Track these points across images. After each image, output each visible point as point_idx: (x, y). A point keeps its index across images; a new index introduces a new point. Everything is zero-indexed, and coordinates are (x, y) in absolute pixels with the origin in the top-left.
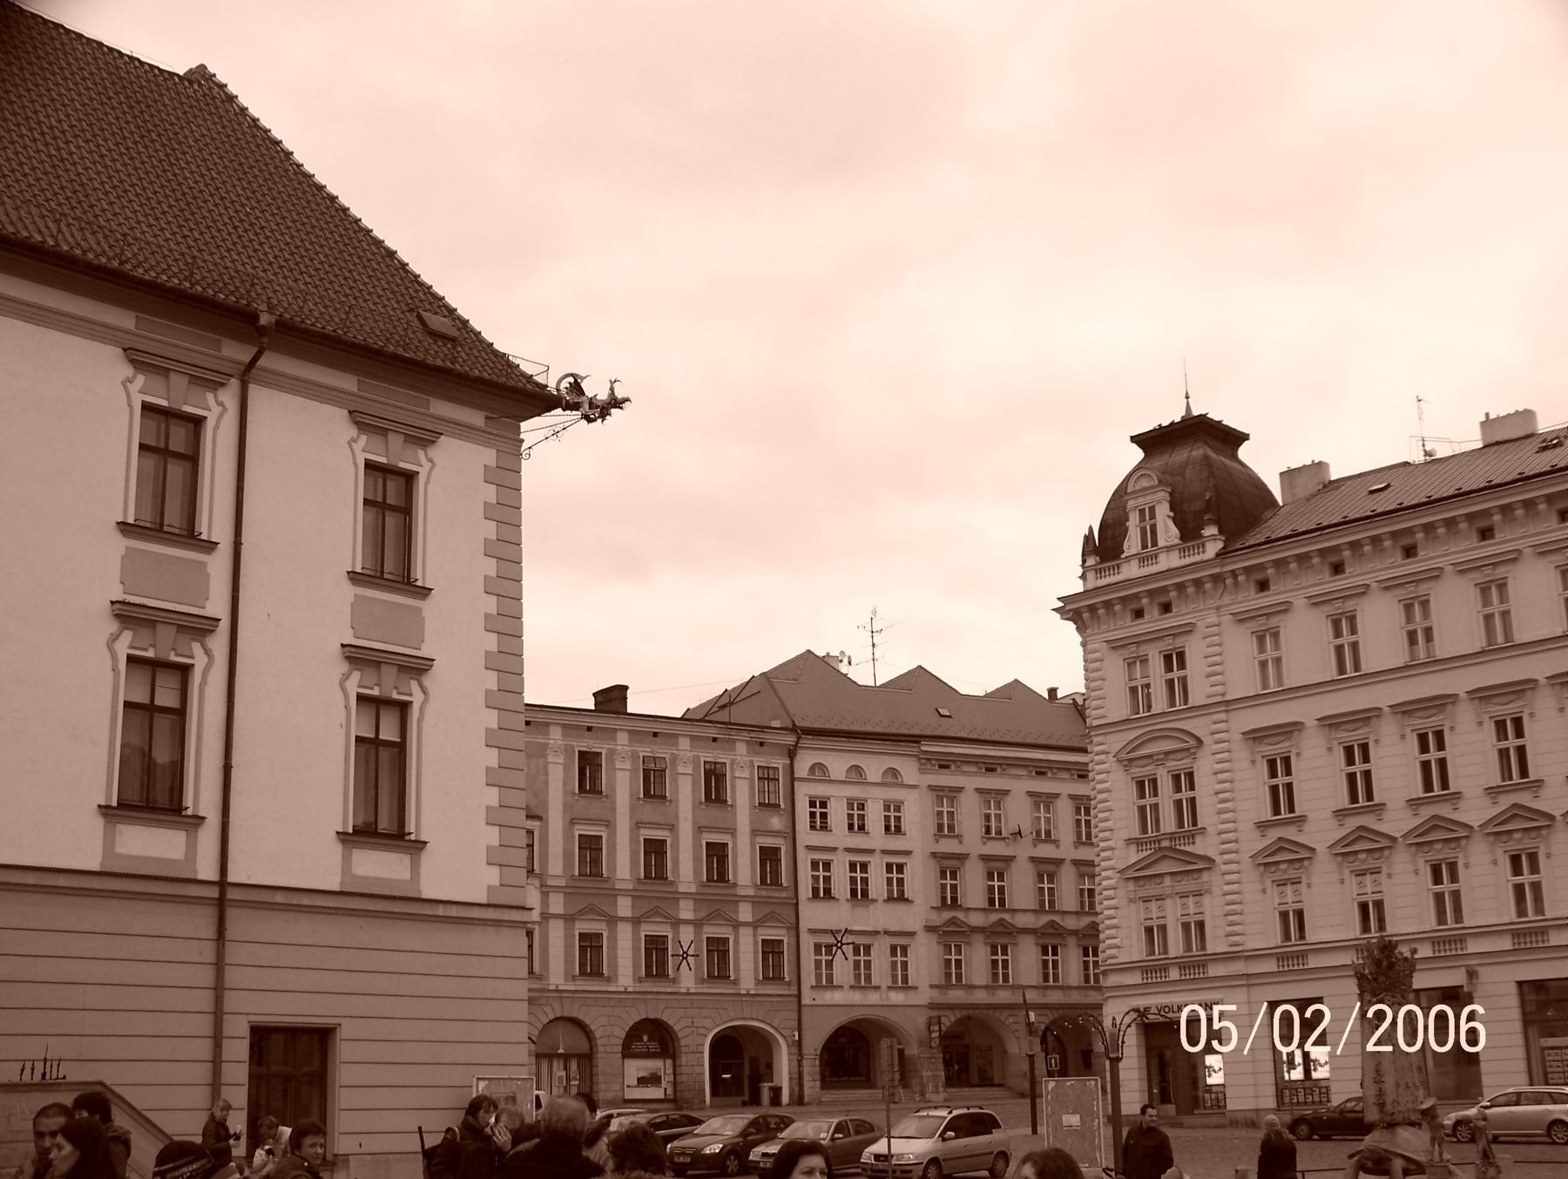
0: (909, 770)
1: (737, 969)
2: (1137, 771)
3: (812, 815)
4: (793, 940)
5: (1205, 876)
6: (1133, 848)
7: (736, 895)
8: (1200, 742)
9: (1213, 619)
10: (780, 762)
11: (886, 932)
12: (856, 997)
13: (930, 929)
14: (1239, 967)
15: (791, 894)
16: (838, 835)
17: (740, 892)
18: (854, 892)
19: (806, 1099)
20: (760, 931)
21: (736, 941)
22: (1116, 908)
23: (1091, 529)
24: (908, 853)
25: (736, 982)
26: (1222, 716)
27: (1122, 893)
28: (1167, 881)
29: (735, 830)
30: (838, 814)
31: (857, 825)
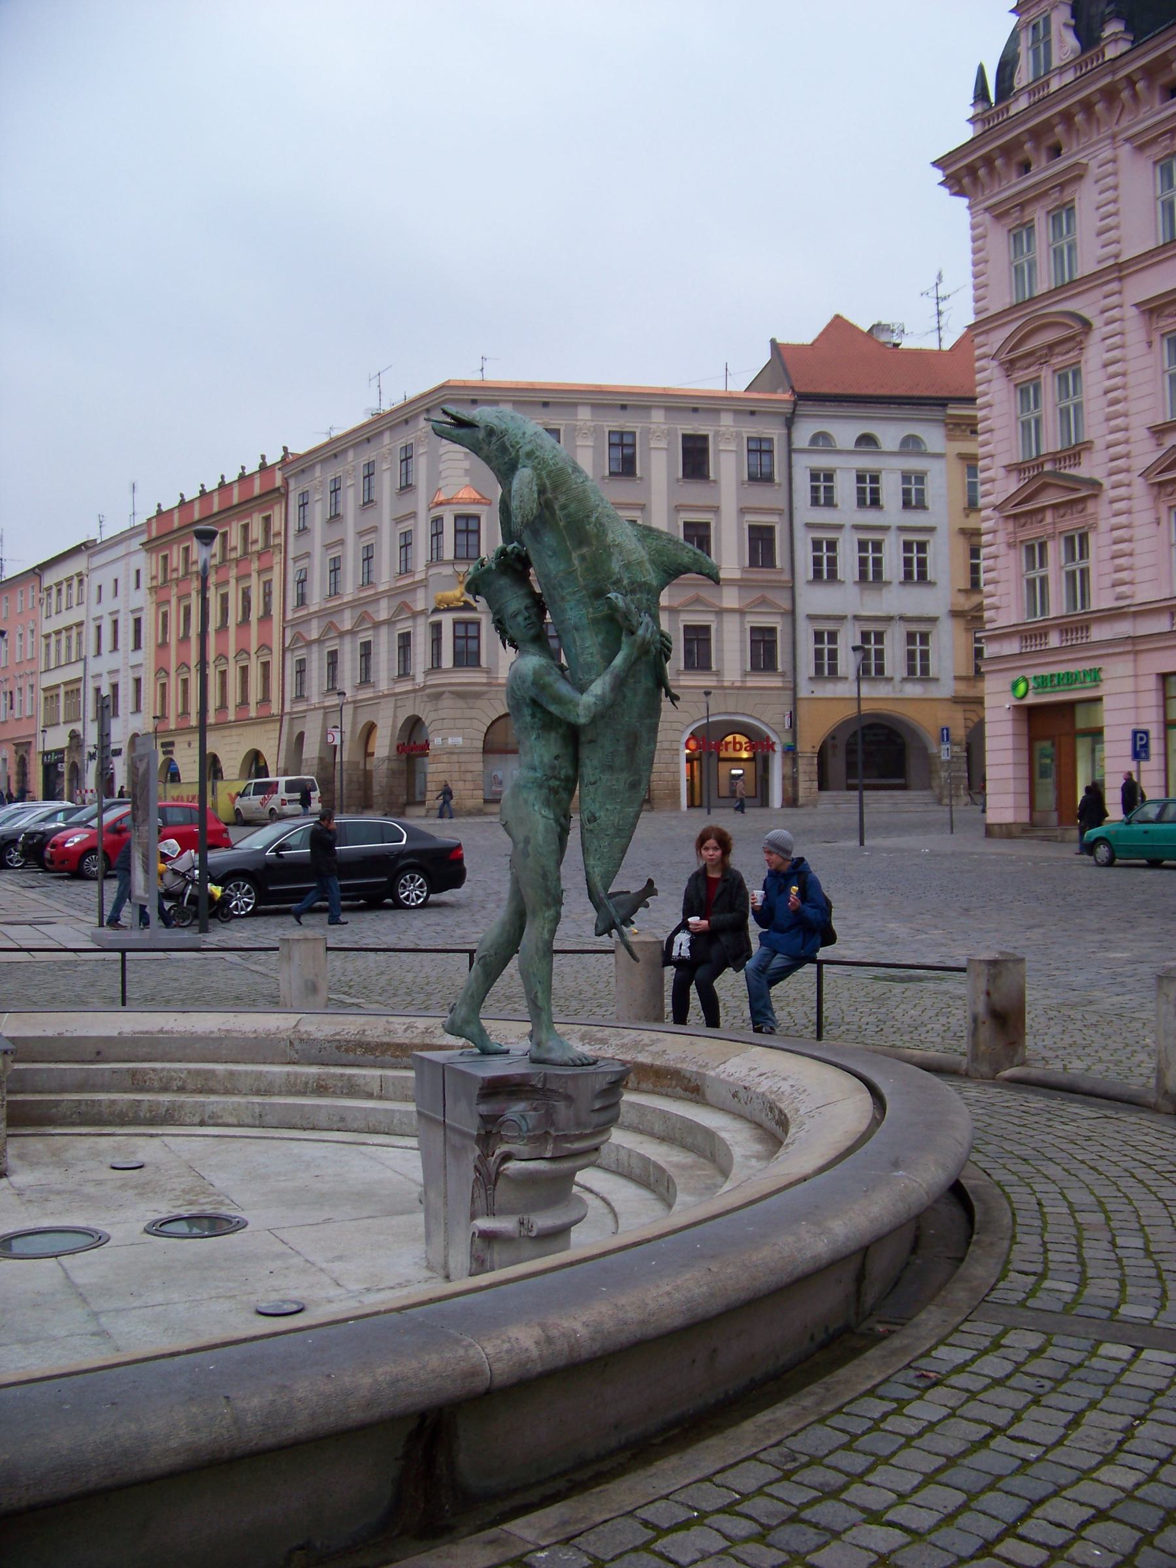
0: (933, 437)
1: (721, 660)
2: (1020, 375)
3: (815, 489)
4: (789, 629)
5: (1091, 507)
6: (1014, 476)
8: (1087, 325)
9: (1107, 154)
10: (774, 431)
11: (902, 618)
13: (955, 614)
14: (1124, 628)
15: (786, 577)
16: (846, 509)
18: (863, 575)
19: (801, 801)
21: (720, 631)
22: (996, 557)
23: (981, 71)
24: (931, 530)
25: (718, 673)
26: (1114, 286)
27: (1001, 537)
28: (1049, 517)
30: (845, 488)
31: (870, 498)
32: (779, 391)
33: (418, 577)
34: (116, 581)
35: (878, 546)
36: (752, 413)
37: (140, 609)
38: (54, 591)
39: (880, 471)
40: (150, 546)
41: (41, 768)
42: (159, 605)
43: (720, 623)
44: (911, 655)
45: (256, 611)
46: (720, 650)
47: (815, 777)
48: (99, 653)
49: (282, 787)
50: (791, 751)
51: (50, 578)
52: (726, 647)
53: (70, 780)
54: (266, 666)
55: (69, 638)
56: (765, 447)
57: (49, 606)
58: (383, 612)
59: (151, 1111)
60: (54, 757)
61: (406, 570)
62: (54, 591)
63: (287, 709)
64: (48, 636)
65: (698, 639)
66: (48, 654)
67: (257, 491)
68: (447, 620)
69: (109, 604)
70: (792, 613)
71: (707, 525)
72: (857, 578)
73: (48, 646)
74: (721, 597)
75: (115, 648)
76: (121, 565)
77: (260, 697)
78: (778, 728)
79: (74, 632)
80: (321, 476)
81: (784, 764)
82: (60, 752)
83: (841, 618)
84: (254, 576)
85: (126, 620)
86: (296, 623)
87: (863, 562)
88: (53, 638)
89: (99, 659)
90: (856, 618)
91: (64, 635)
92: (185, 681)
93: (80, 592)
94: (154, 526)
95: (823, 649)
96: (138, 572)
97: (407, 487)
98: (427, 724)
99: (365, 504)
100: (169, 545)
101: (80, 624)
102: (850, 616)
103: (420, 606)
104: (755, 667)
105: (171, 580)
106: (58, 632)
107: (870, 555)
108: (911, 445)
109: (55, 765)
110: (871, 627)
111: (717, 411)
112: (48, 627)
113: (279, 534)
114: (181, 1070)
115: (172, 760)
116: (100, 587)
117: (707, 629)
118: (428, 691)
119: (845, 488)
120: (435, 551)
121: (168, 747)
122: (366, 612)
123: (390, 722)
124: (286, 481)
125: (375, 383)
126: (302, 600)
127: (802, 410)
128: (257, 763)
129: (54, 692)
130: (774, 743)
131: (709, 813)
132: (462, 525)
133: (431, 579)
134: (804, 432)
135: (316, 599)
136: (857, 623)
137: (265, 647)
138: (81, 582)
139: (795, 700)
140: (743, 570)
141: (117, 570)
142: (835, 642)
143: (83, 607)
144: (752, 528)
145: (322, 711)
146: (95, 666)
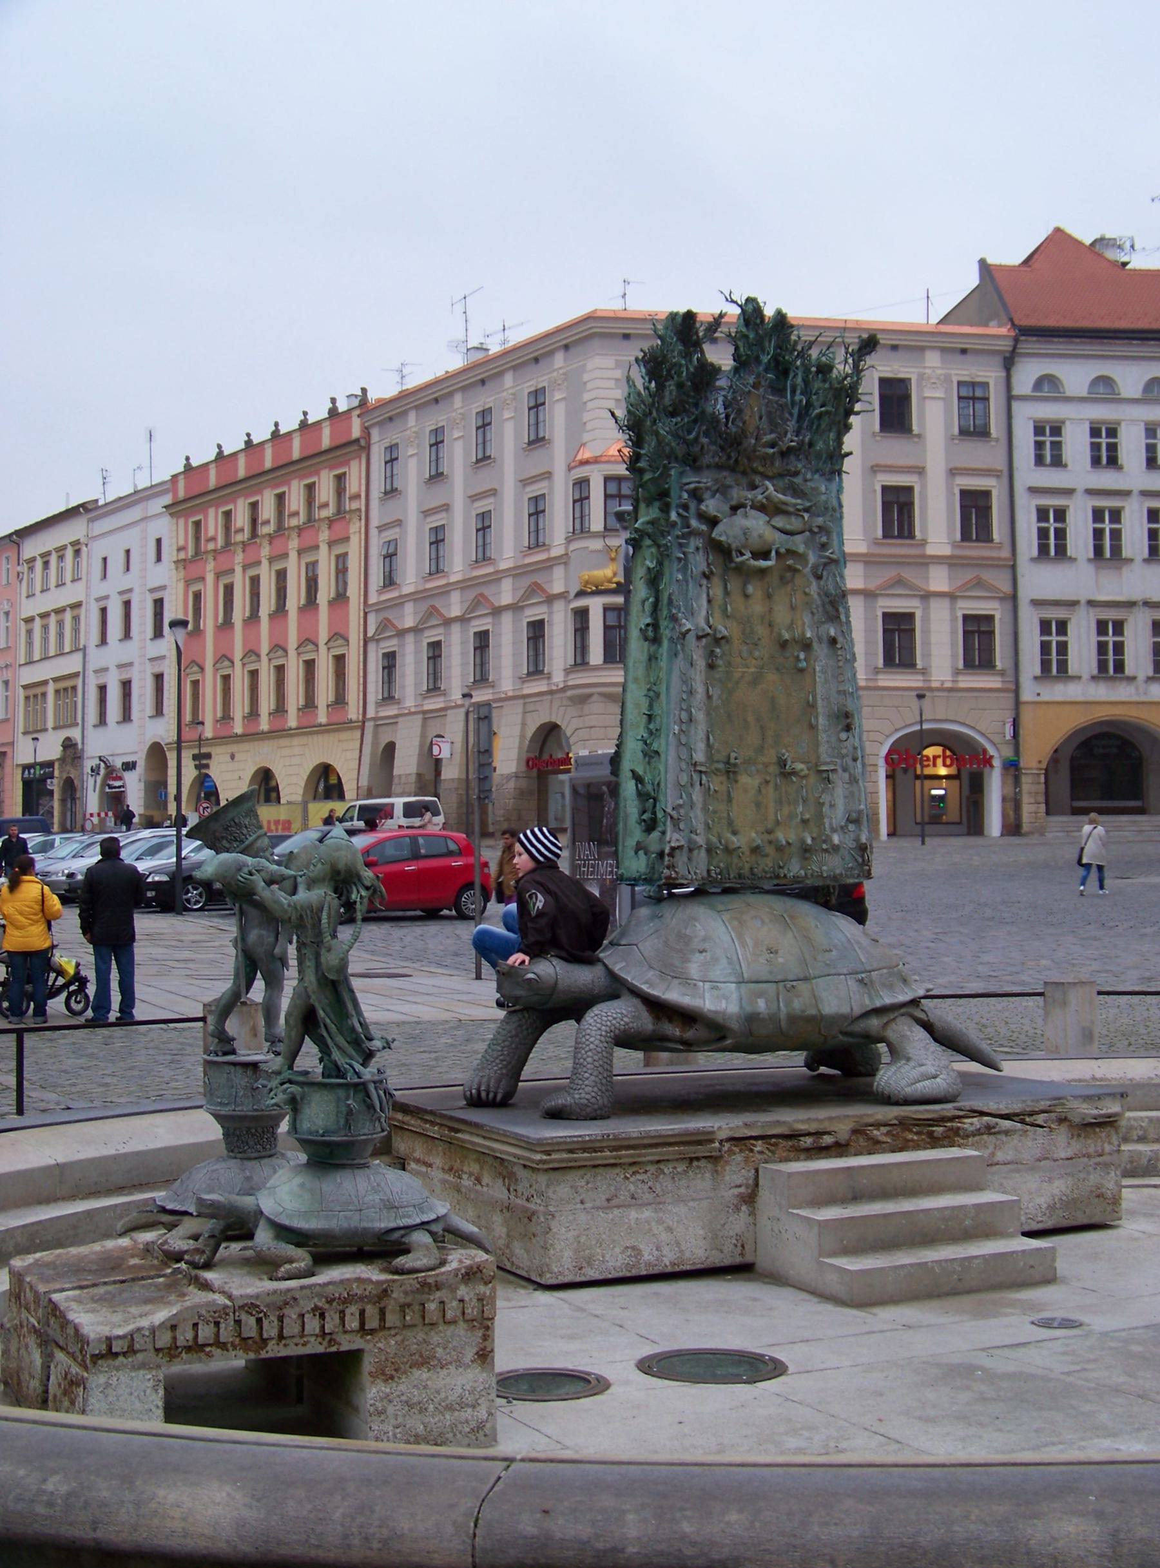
1: (927, 655)
3: (1039, 445)
4: (1009, 618)
7: (924, 556)
10: (990, 374)
11: (1146, 604)
12: (1101, 692)
15: (1006, 553)
17: (930, 550)
18: (1098, 550)
19: (1025, 827)
20: (961, 604)
21: (926, 619)
25: (924, 672)
29: (923, 468)
30: (1077, 444)
32: (992, 324)
33: (556, 552)
34: (128, 552)
35: (1116, 515)
36: (964, 351)
37: (163, 588)
38: (39, 564)
39: (1118, 423)
40: (175, 509)
41: (20, 785)
42: (188, 583)
43: (926, 610)
44: (1102, 648)
45: (325, 593)
46: (927, 643)
47: (1042, 799)
48: (103, 641)
49: (399, 811)
50: (1013, 767)
51: (32, 548)
52: (934, 638)
53: (63, 801)
54: (340, 660)
55: (60, 624)
56: (979, 393)
57: (31, 582)
58: (506, 594)
59: (1132, 1162)
60: (39, 772)
61: (537, 543)
62: (39, 564)
63: (371, 713)
64: (29, 620)
65: (899, 630)
66: (30, 643)
67: (326, 442)
68: (596, 606)
69: (118, 580)
70: (1014, 598)
71: (909, 490)
72: (1091, 555)
73: (29, 632)
74: (927, 579)
75: (127, 634)
76: (135, 532)
77: (331, 698)
78: (997, 739)
79: (68, 616)
80: (418, 428)
81: (1004, 783)
82: (50, 764)
83: (1074, 604)
84: (324, 548)
85: (143, 601)
86: (380, 608)
87: (1098, 534)
88: (38, 622)
89: (104, 649)
90: (1091, 603)
91: (53, 619)
92: (226, 679)
93: (77, 566)
94: (181, 483)
95: (1107, 643)
96: (159, 542)
97: (537, 441)
98: (568, 733)
99: (478, 461)
100: (205, 509)
101: (77, 606)
102: (1083, 601)
103: (557, 588)
104: (969, 664)
105: (206, 552)
106: (44, 616)
107: (1107, 526)
108: (1104, 389)
109: (43, 780)
110: (1111, 615)
111: (922, 349)
112: (30, 608)
113: (358, 496)
114: (1141, 1118)
115: (207, 776)
116: (105, 559)
117: (910, 617)
118: (570, 693)
119: (1077, 444)
120: (578, 522)
121: (202, 760)
122: (481, 595)
123: (517, 731)
124: (366, 431)
125: (459, 308)
126: (390, 581)
127: (1024, 348)
128: (326, 780)
129: (39, 691)
130: (992, 757)
131: (923, 843)
132: (612, 489)
133: (572, 555)
134: (1026, 375)
135: (411, 577)
136: (1092, 611)
137: (338, 636)
138: (77, 552)
139: (1018, 703)
140: (954, 545)
141: (131, 539)
142: (1065, 633)
143: (81, 586)
144: (964, 493)
145: (420, 716)
146: (97, 658)
